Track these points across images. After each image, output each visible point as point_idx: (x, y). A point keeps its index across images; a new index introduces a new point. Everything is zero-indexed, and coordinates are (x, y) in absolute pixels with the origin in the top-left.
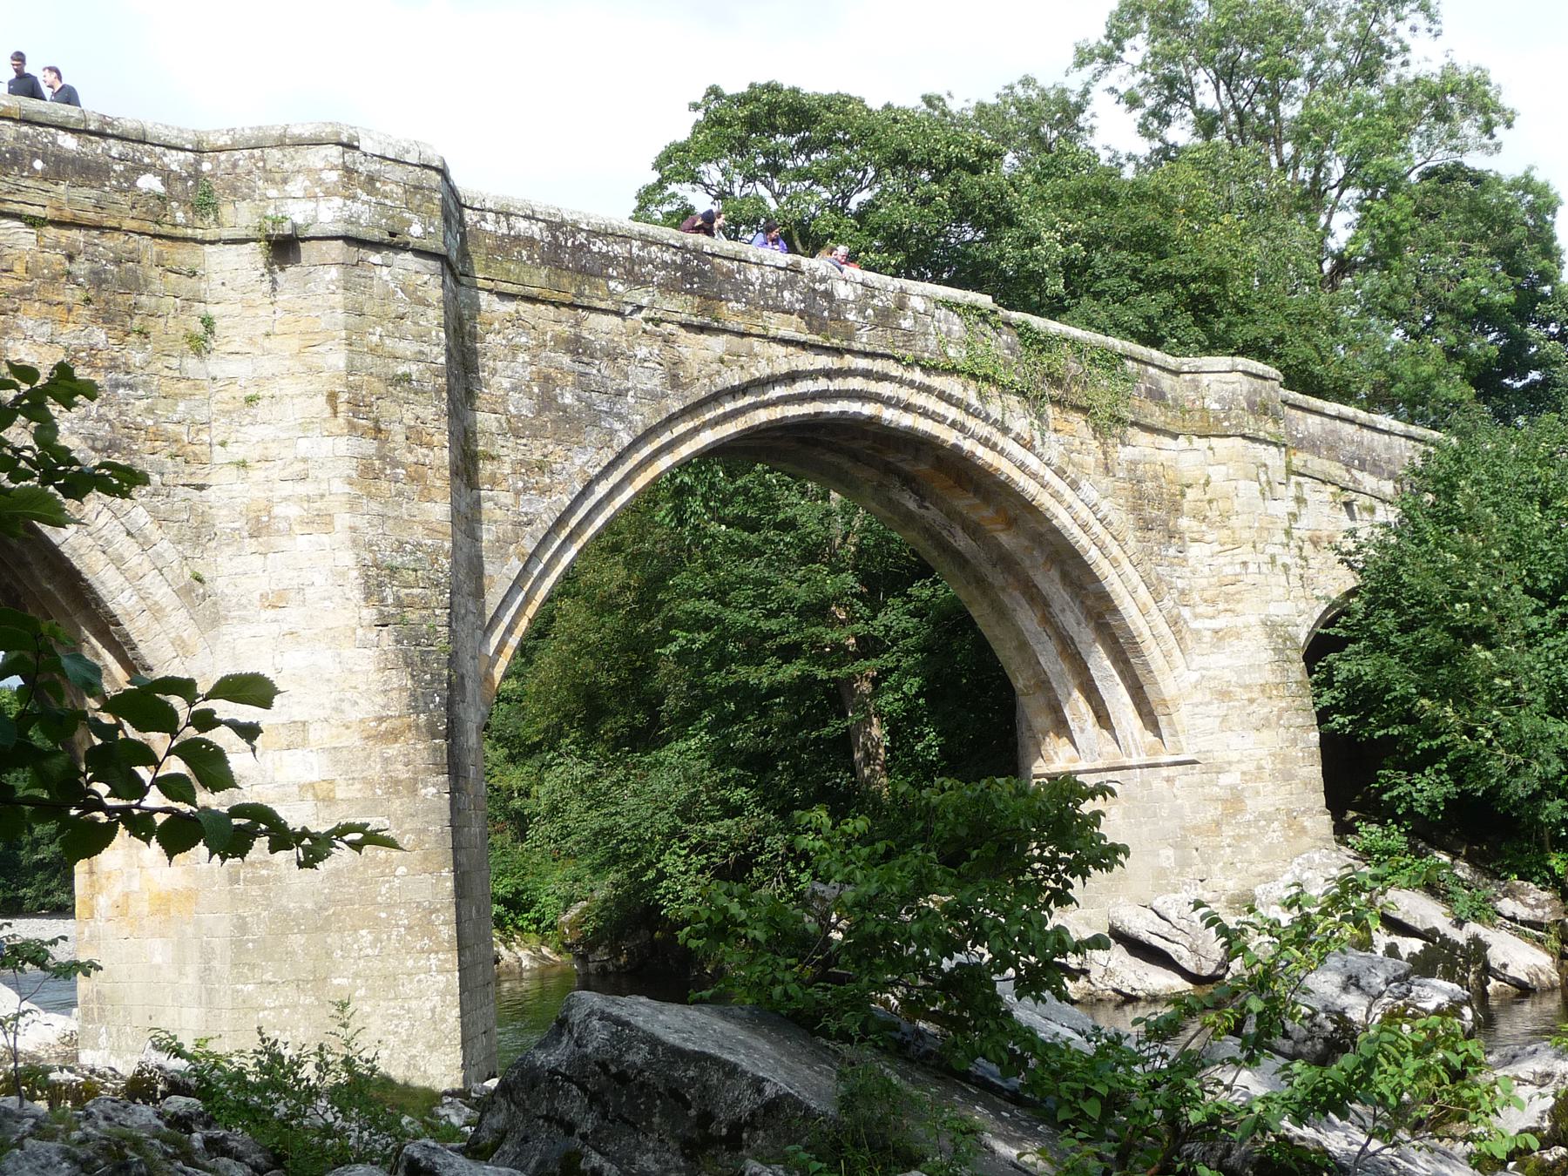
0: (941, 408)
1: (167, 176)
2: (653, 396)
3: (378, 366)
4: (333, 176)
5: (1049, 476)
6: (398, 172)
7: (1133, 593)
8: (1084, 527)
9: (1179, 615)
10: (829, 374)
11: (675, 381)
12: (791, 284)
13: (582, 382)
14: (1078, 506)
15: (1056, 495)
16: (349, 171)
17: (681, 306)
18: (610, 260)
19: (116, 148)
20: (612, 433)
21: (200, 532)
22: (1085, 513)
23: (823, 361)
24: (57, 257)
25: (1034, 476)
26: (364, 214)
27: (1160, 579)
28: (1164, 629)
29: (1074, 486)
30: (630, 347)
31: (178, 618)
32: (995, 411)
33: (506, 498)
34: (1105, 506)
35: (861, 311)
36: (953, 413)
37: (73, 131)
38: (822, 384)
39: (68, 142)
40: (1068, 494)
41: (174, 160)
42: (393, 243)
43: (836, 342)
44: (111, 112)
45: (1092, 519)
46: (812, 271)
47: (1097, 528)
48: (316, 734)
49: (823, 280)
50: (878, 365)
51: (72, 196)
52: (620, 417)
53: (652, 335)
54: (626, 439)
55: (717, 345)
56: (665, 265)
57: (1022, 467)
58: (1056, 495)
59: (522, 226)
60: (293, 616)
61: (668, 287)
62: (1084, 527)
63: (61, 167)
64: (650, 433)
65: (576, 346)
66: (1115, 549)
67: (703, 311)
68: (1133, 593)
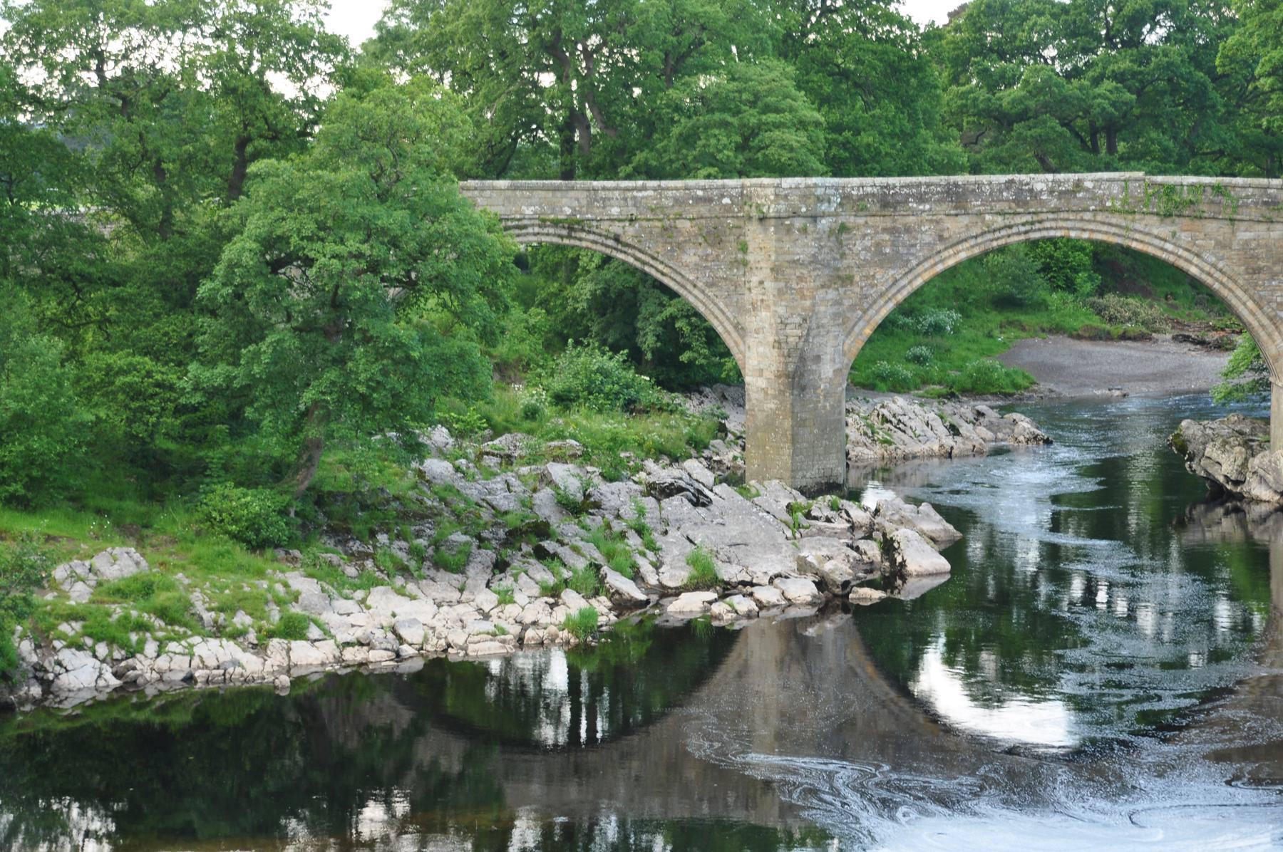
0: (1105, 228)
1: (731, 197)
2: (929, 244)
3: (788, 258)
4: (772, 197)
5: (1181, 252)
6: (798, 192)
7: (1244, 304)
8: (1209, 274)
9: (1276, 315)
10: (1032, 223)
11: (941, 238)
12: (1008, 189)
13: (894, 244)
14: (1202, 264)
15: (1187, 260)
16: (776, 195)
17: (946, 207)
18: (908, 195)
20: (908, 261)
21: (741, 309)
22: (1207, 268)
23: (1029, 218)
24: (696, 229)
25: (1172, 253)
26: (782, 206)
27: (1261, 298)
28: (1266, 322)
29: (1198, 255)
30: (920, 227)
31: (735, 335)
32: (1138, 226)
33: (857, 290)
34: (1221, 265)
35: (1051, 192)
36: (1113, 230)
38: (1028, 227)
39: (700, 193)
40: (1196, 260)
41: (733, 193)
42: (796, 214)
43: (1032, 210)
45: (1213, 271)
46: (1021, 183)
47: (1217, 275)
48: (767, 374)
49: (1027, 184)
50: (1062, 215)
51: (703, 209)
52: (913, 255)
53: (931, 221)
54: (914, 262)
55: (964, 220)
56: (938, 193)
57: (1162, 249)
58: (1187, 260)
59: (869, 189)
60: (761, 336)
61: (939, 201)
62: (1209, 274)
63: (698, 200)
64: (926, 259)
65: (892, 231)
66: (1231, 285)
67: (956, 208)
68: (1244, 304)
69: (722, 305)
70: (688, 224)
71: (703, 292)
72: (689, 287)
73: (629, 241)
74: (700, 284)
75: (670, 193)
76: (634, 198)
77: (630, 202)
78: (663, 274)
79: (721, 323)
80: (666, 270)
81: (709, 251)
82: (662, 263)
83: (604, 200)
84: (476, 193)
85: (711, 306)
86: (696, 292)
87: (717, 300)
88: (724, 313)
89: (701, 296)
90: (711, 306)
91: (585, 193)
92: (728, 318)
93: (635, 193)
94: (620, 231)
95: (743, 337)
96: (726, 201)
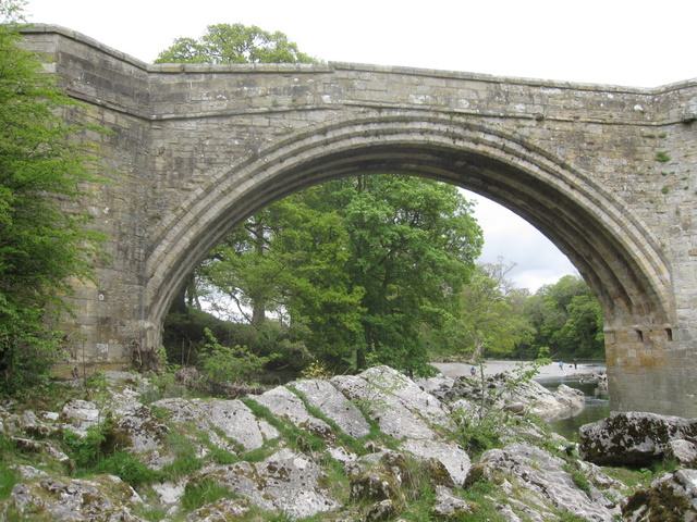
19: (627, 97)
31: (657, 260)
37: (612, 92)
41: (645, 99)
44: (622, 85)
63: (610, 103)
69: (643, 224)
70: (597, 130)
71: (621, 209)
72: (604, 202)
73: (538, 144)
74: (618, 199)
75: (579, 94)
76: (541, 95)
77: (537, 100)
78: (573, 187)
79: (640, 247)
80: (578, 182)
81: (625, 162)
82: (573, 172)
83: (507, 94)
84: (352, 74)
85: (630, 226)
86: (612, 208)
87: (637, 218)
88: (644, 233)
89: (618, 214)
90: (630, 226)
91: (485, 85)
92: (650, 241)
93: (541, 90)
94: (525, 132)
95: (665, 262)
96: (637, 107)
